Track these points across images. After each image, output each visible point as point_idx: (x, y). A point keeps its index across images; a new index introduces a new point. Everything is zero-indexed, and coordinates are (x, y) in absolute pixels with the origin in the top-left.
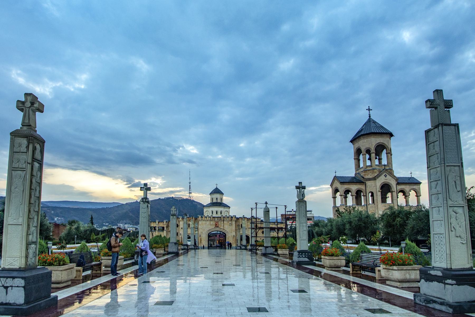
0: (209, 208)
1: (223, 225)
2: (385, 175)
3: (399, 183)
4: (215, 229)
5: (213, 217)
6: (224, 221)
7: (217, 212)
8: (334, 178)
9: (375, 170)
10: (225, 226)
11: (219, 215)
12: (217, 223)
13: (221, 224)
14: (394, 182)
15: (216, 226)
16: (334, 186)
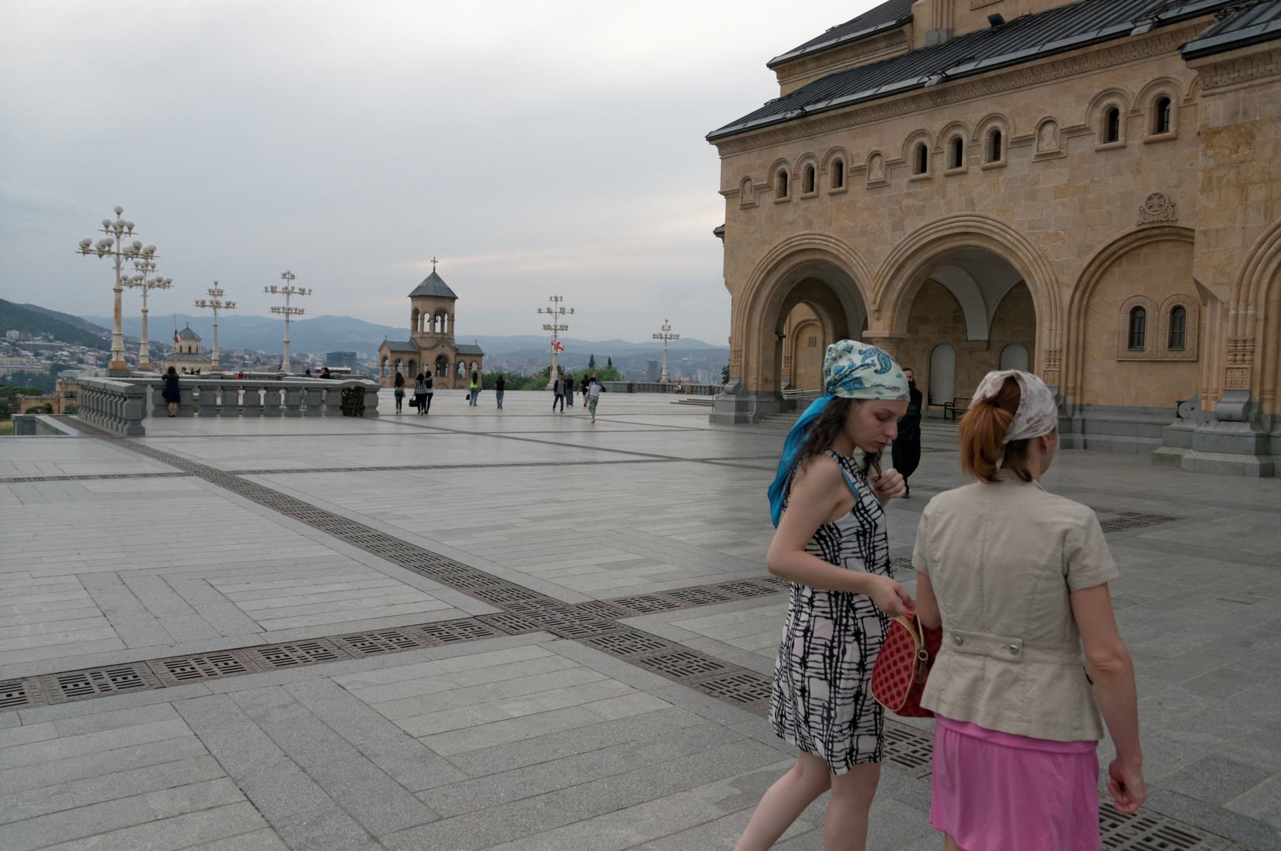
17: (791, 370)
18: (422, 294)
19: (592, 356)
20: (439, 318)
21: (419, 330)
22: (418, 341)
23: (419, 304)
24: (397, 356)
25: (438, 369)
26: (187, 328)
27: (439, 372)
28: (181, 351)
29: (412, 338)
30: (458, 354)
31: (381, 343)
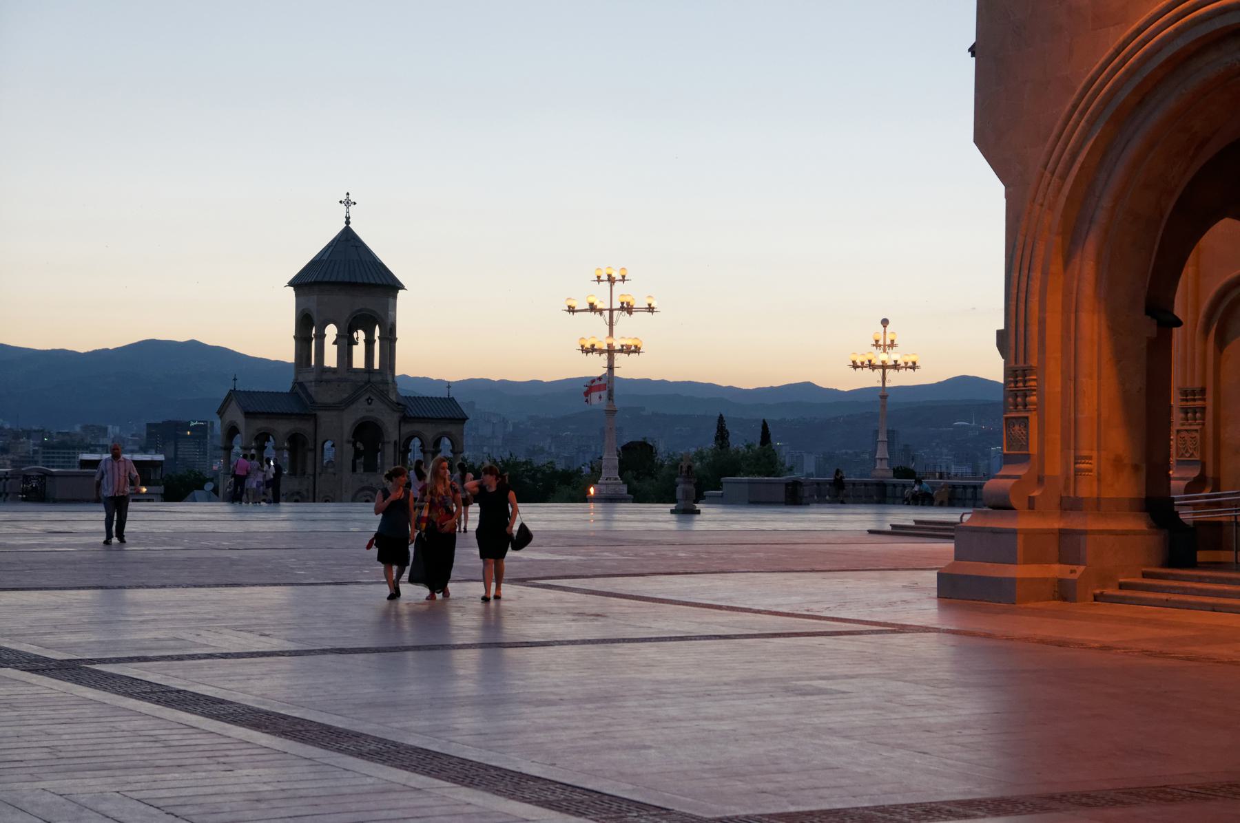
2: (368, 400)
8: (229, 395)
17: (1203, 437)
18: (319, 279)
19: (721, 419)
20: (361, 335)
22: (312, 389)
23: (312, 302)
24: (261, 424)
25: (358, 453)
29: (298, 384)
30: (405, 419)
31: (226, 394)
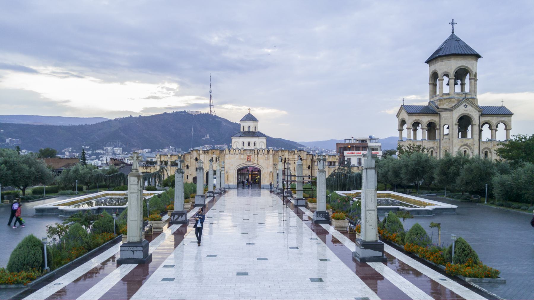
0: (239, 138)
1: (256, 159)
2: (465, 106)
3: (483, 114)
4: (246, 164)
5: (244, 150)
6: (258, 154)
7: (249, 144)
8: (401, 107)
9: (453, 100)
10: (259, 160)
11: (252, 147)
12: (249, 157)
13: (254, 158)
14: (476, 114)
15: (248, 160)
16: (401, 117)
21: (438, 93)
24: (415, 118)
26: (249, 113)
27: (460, 133)
28: (244, 130)
